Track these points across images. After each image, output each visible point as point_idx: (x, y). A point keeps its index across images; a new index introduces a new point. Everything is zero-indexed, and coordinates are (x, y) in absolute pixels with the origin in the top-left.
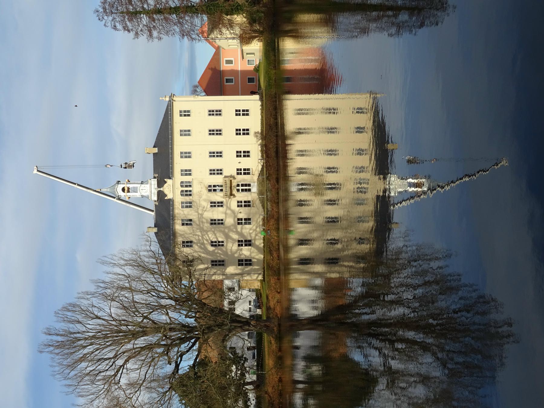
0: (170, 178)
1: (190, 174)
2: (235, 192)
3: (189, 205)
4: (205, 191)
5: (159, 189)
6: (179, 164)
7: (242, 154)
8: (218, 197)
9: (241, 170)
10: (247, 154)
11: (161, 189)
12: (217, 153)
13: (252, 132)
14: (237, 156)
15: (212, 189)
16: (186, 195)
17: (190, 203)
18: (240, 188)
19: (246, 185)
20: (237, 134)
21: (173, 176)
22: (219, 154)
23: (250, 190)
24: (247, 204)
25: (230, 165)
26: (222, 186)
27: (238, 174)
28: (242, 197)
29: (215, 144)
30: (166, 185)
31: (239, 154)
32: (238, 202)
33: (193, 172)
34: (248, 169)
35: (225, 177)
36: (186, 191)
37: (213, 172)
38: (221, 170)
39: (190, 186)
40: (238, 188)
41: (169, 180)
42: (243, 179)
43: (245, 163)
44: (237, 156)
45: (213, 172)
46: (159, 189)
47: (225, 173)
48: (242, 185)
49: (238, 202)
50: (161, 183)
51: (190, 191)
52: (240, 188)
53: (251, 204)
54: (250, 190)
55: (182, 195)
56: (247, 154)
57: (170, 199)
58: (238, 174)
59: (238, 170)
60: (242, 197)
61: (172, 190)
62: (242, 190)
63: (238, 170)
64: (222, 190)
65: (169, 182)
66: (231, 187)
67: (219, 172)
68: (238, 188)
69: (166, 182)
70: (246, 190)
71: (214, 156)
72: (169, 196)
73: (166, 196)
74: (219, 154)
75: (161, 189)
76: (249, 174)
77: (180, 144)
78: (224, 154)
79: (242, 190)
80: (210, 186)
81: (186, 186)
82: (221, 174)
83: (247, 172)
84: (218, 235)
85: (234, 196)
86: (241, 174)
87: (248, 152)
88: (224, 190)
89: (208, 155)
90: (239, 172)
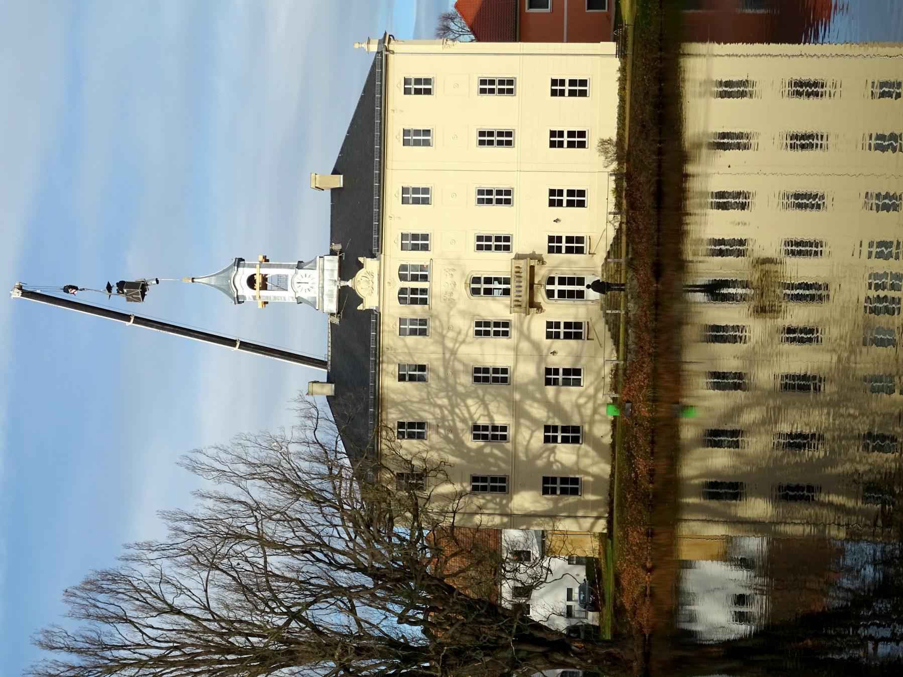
2: (541, 297)
27: (551, 250)
32: (549, 325)
33: (433, 243)
35: (519, 257)
36: (414, 291)
37: (484, 243)
39: (425, 278)
40: (550, 287)
45: (484, 243)
49: (549, 325)
51: (424, 291)
52: (556, 287)
58: (551, 250)
62: (562, 294)
68: (550, 287)
79: (562, 294)
81: (415, 278)
84: (493, 407)
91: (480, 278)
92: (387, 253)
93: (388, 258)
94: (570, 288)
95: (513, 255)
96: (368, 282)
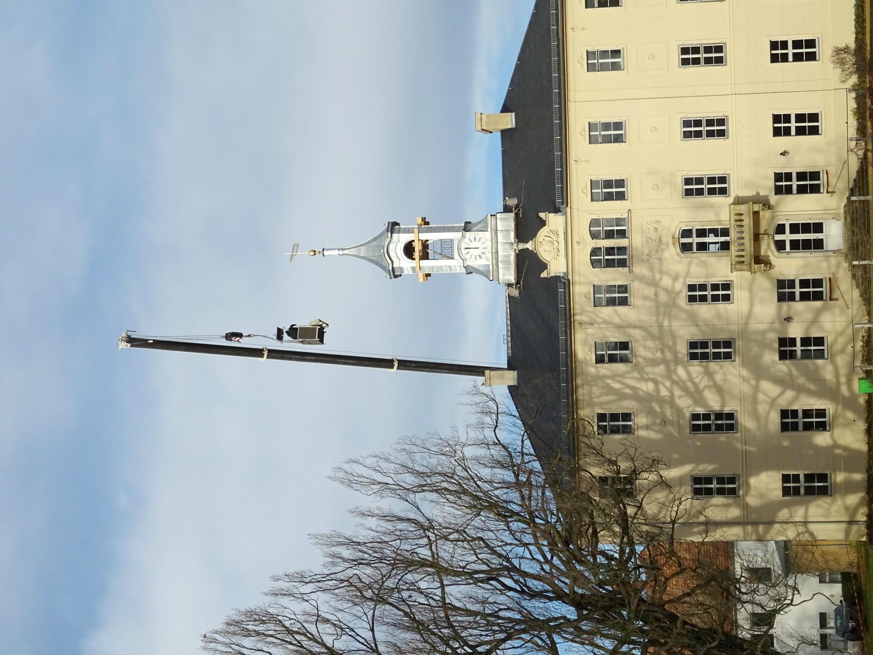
0: (557, 211)
1: (621, 196)
3: (619, 297)
4: (672, 252)
5: (522, 246)
6: (586, 162)
7: (793, 125)
8: (716, 267)
9: (788, 177)
10: (809, 124)
11: (529, 246)
12: (710, 122)
13: (824, 50)
14: (777, 132)
15: (693, 241)
16: (610, 264)
17: (623, 289)
18: (788, 237)
19: (807, 228)
20: (774, 59)
21: (565, 201)
22: (716, 128)
23: (818, 245)
24: (813, 290)
25: (749, 158)
26: (725, 232)
27: (778, 190)
28: (792, 265)
29: (704, 92)
30: (543, 233)
31: (781, 125)
32: (781, 284)
33: (630, 189)
34: (815, 175)
35: (739, 201)
36: (610, 251)
37: (695, 187)
38: (723, 180)
39: (622, 234)
40: (779, 237)
41: (551, 216)
42: (798, 208)
43: (803, 154)
44: (777, 132)
46: (522, 246)
47: (736, 189)
48: (795, 228)
50: (526, 228)
51: (622, 250)
52: (788, 237)
53: (825, 289)
54: (818, 245)
55: (594, 264)
56: (809, 124)
57: (557, 278)
58: (778, 190)
59: (778, 177)
60: (792, 265)
61: (563, 245)
62: (795, 245)
63: (778, 177)
64: (725, 246)
65: (554, 221)
66: (757, 237)
67: (717, 185)
68: (779, 237)
69: (543, 223)
70: (807, 245)
71: (698, 134)
72: (556, 267)
73: (544, 266)
74: (716, 128)
75: (529, 246)
76: (815, 189)
77: (588, 98)
78: (731, 127)
79: (795, 245)
80: (687, 233)
81: (609, 235)
82: (723, 192)
83: (810, 182)
85: (768, 263)
86: (789, 190)
87: (814, 117)
88: (733, 248)
89: (679, 129)
90: (784, 184)
91: (690, 231)
92: (575, 206)
93: (575, 212)
94: (807, 237)
95: (730, 200)
96: (552, 243)
